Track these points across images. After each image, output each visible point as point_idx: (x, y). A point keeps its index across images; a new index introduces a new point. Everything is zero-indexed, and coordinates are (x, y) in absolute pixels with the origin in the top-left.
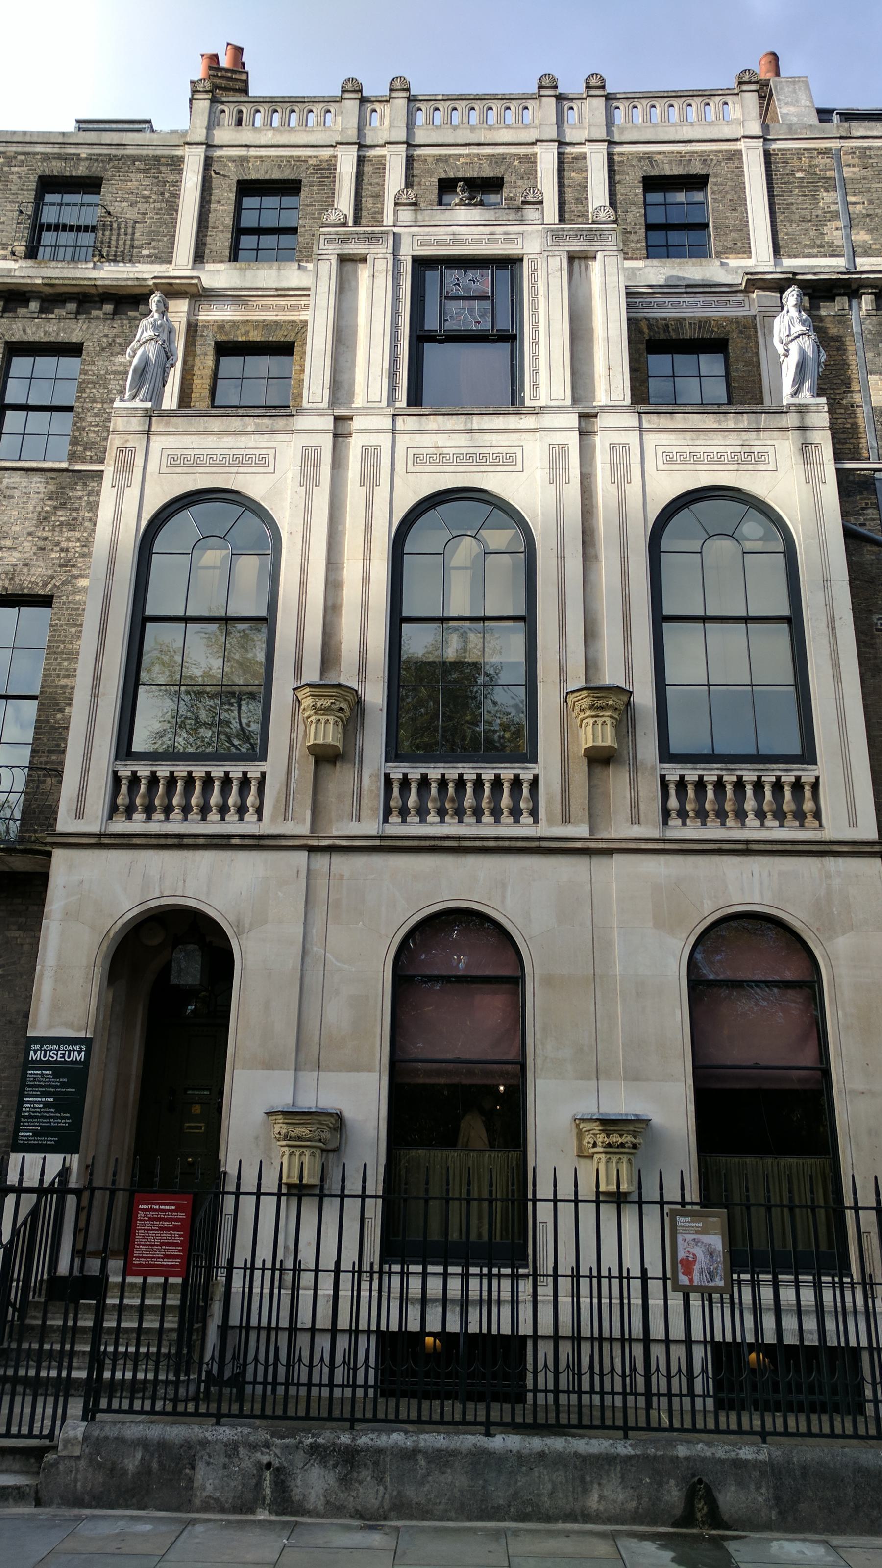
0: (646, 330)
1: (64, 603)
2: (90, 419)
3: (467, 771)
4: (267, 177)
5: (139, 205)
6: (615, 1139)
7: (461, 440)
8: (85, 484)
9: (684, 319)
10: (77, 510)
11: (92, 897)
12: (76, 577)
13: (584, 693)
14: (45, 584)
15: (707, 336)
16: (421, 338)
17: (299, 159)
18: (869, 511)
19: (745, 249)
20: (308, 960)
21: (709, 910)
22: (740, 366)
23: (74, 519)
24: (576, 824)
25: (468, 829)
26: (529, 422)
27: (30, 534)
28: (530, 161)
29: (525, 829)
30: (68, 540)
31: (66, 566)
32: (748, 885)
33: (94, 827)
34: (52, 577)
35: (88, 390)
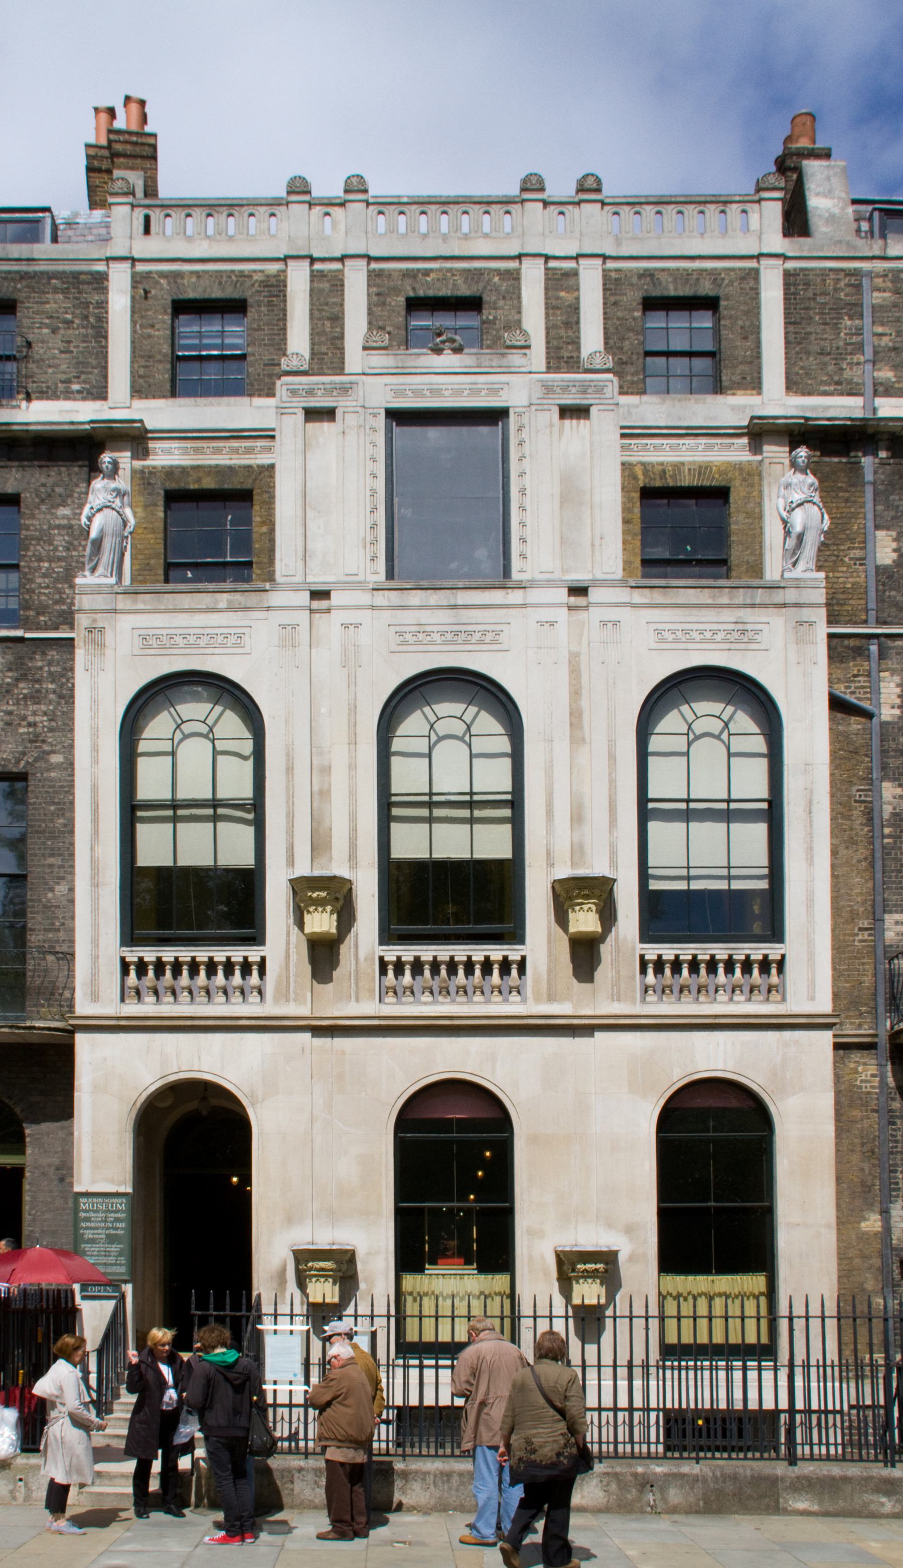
0: (641, 477)
1: (40, 781)
2: (39, 580)
5: (62, 332)
8: (44, 653)
9: (683, 464)
10: (38, 681)
12: (49, 753)
14: (18, 761)
15: (707, 483)
18: (860, 678)
19: (755, 384)
22: (741, 517)
23: (38, 691)
28: (514, 277)
30: (34, 714)
31: (36, 742)
35: (32, 548)
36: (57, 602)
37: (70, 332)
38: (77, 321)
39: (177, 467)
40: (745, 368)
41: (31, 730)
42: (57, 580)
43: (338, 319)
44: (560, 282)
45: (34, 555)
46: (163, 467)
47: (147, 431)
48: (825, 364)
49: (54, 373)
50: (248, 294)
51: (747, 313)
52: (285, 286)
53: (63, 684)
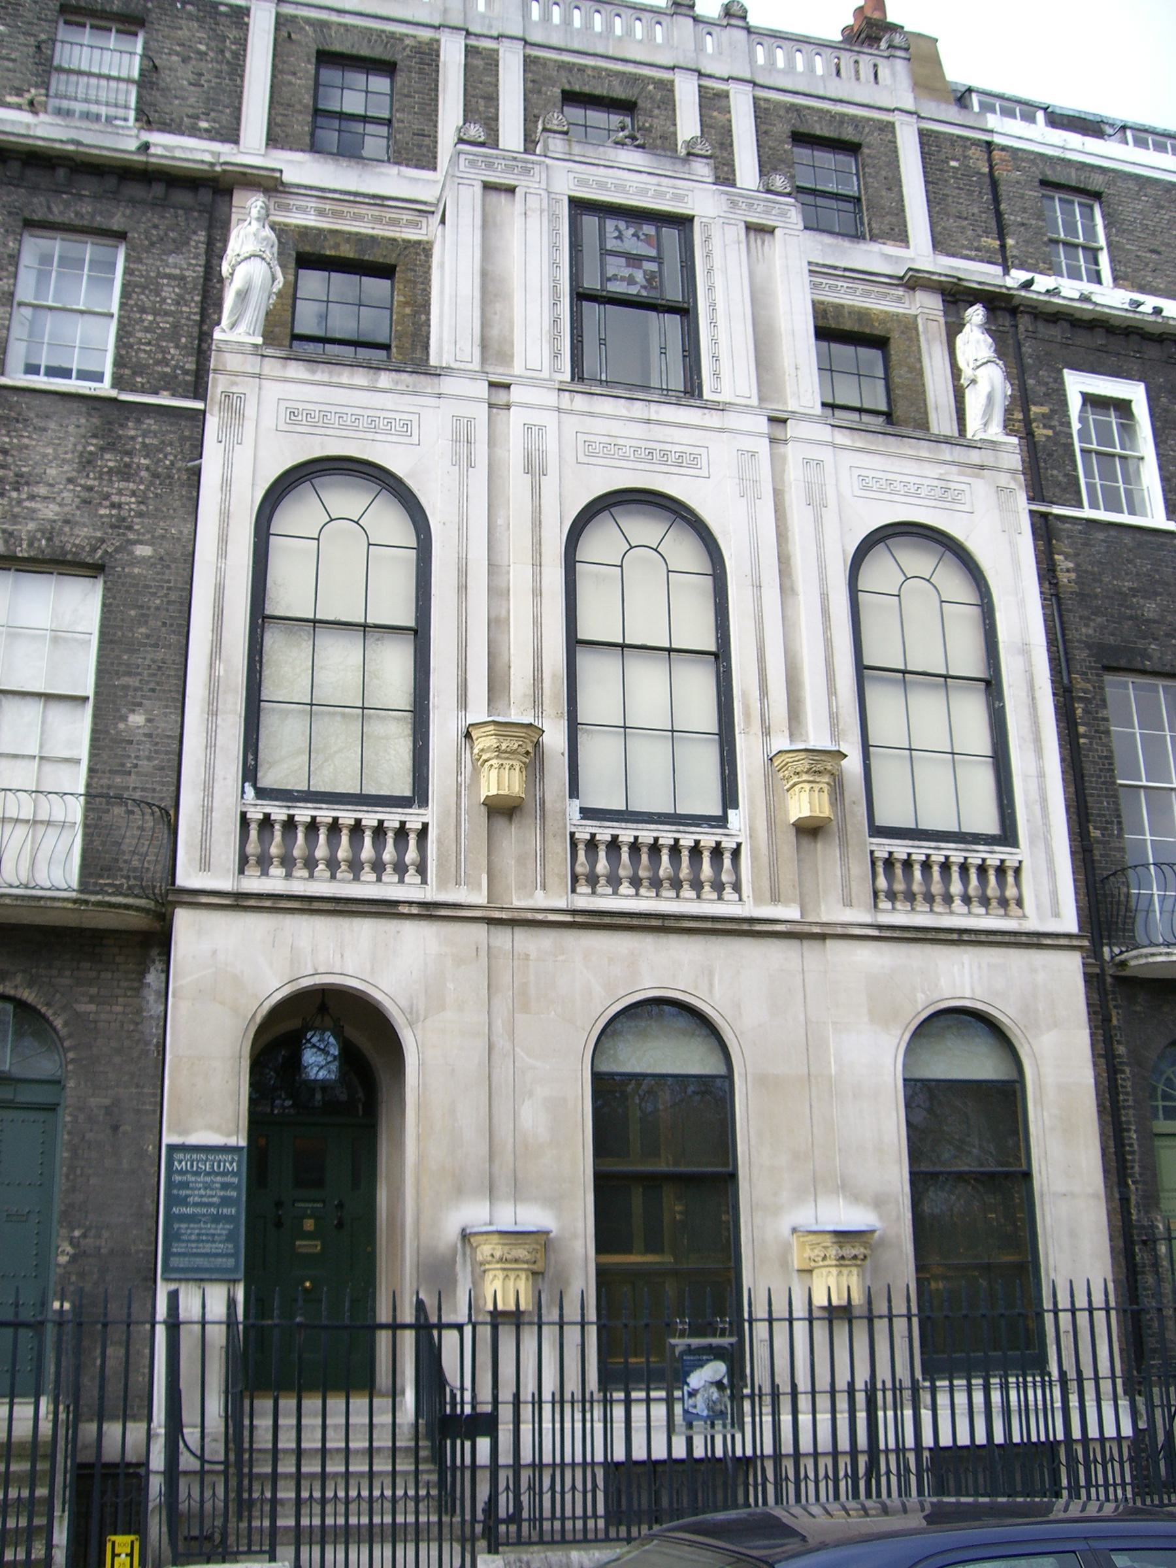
2: (139, 335)
3: (664, 834)
4: (354, 52)
5: (193, 62)
6: (849, 1251)
7: (639, 430)
8: (139, 421)
9: (842, 306)
10: (129, 453)
11: (227, 972)
13: (802, 755)
14: (94, 549)
15: (867, 331)
16: (580, 296)
17: (392, 35)
19: (902, 237)
20: (496, 1056)
21: (921, 1005)
22: (903, 371)
23: (127, 466)
24: (787, 903)
25: (667, 904)
26: (712, 419)
27: (70, 481)
29: (729, 908)
30: (120, 492)
31: (119, 527)
32: (961, 977)
33: (225, 883)
34: (103, 541)
35: (135, 296)
36: (158, 363)
37: (203, 64)
38: (211, 54)
39: (312, 228)
40: (894, 220)
41: (114, 512)
42: (161, 337)
43: (492, 99)
44: (713, 102)
45: (136, 304)
46: (297, 226)
47: (282, 183)
48: (964, 228)
49: (180, 105)
50: (398, 57)
51: (888, 164)
52: (438, 56)
53: (159, 460)
